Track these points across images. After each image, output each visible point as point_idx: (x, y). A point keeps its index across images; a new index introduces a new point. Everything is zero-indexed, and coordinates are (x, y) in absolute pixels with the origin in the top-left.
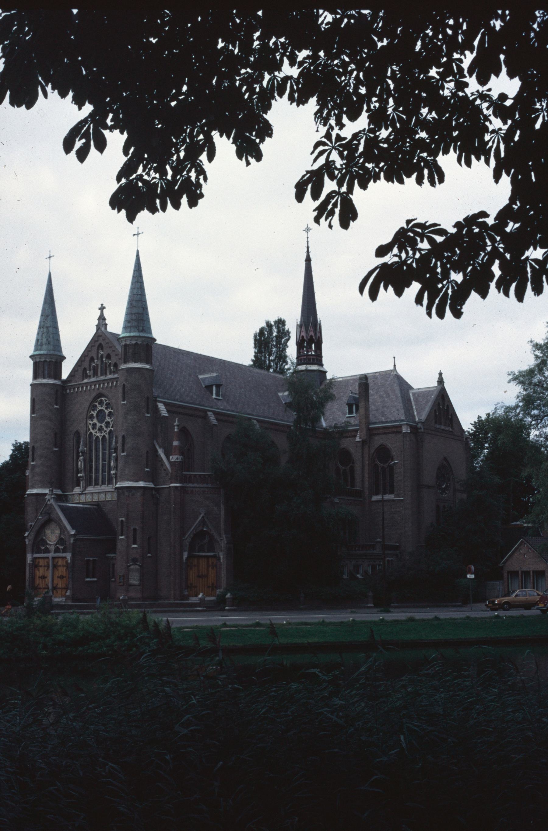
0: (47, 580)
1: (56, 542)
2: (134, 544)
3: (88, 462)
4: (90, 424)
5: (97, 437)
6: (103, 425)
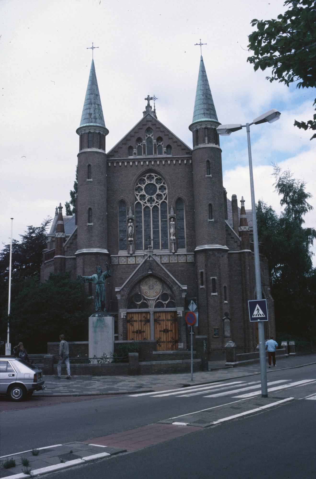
0: (144, 335)
1: (157, 297)
2: (226, 300)
3: (137, 229)
4: (137, 195)
6: (154, 197)
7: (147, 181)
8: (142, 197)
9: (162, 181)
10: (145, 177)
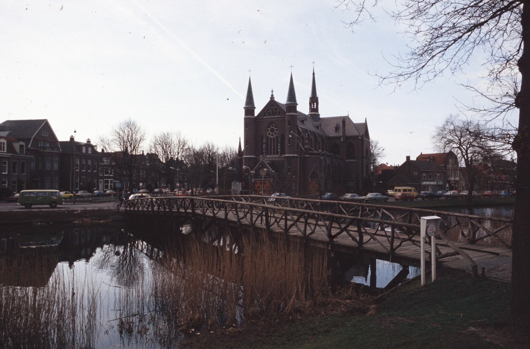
3: (267, 146)
5: (271, 138)
6: (274, 133)
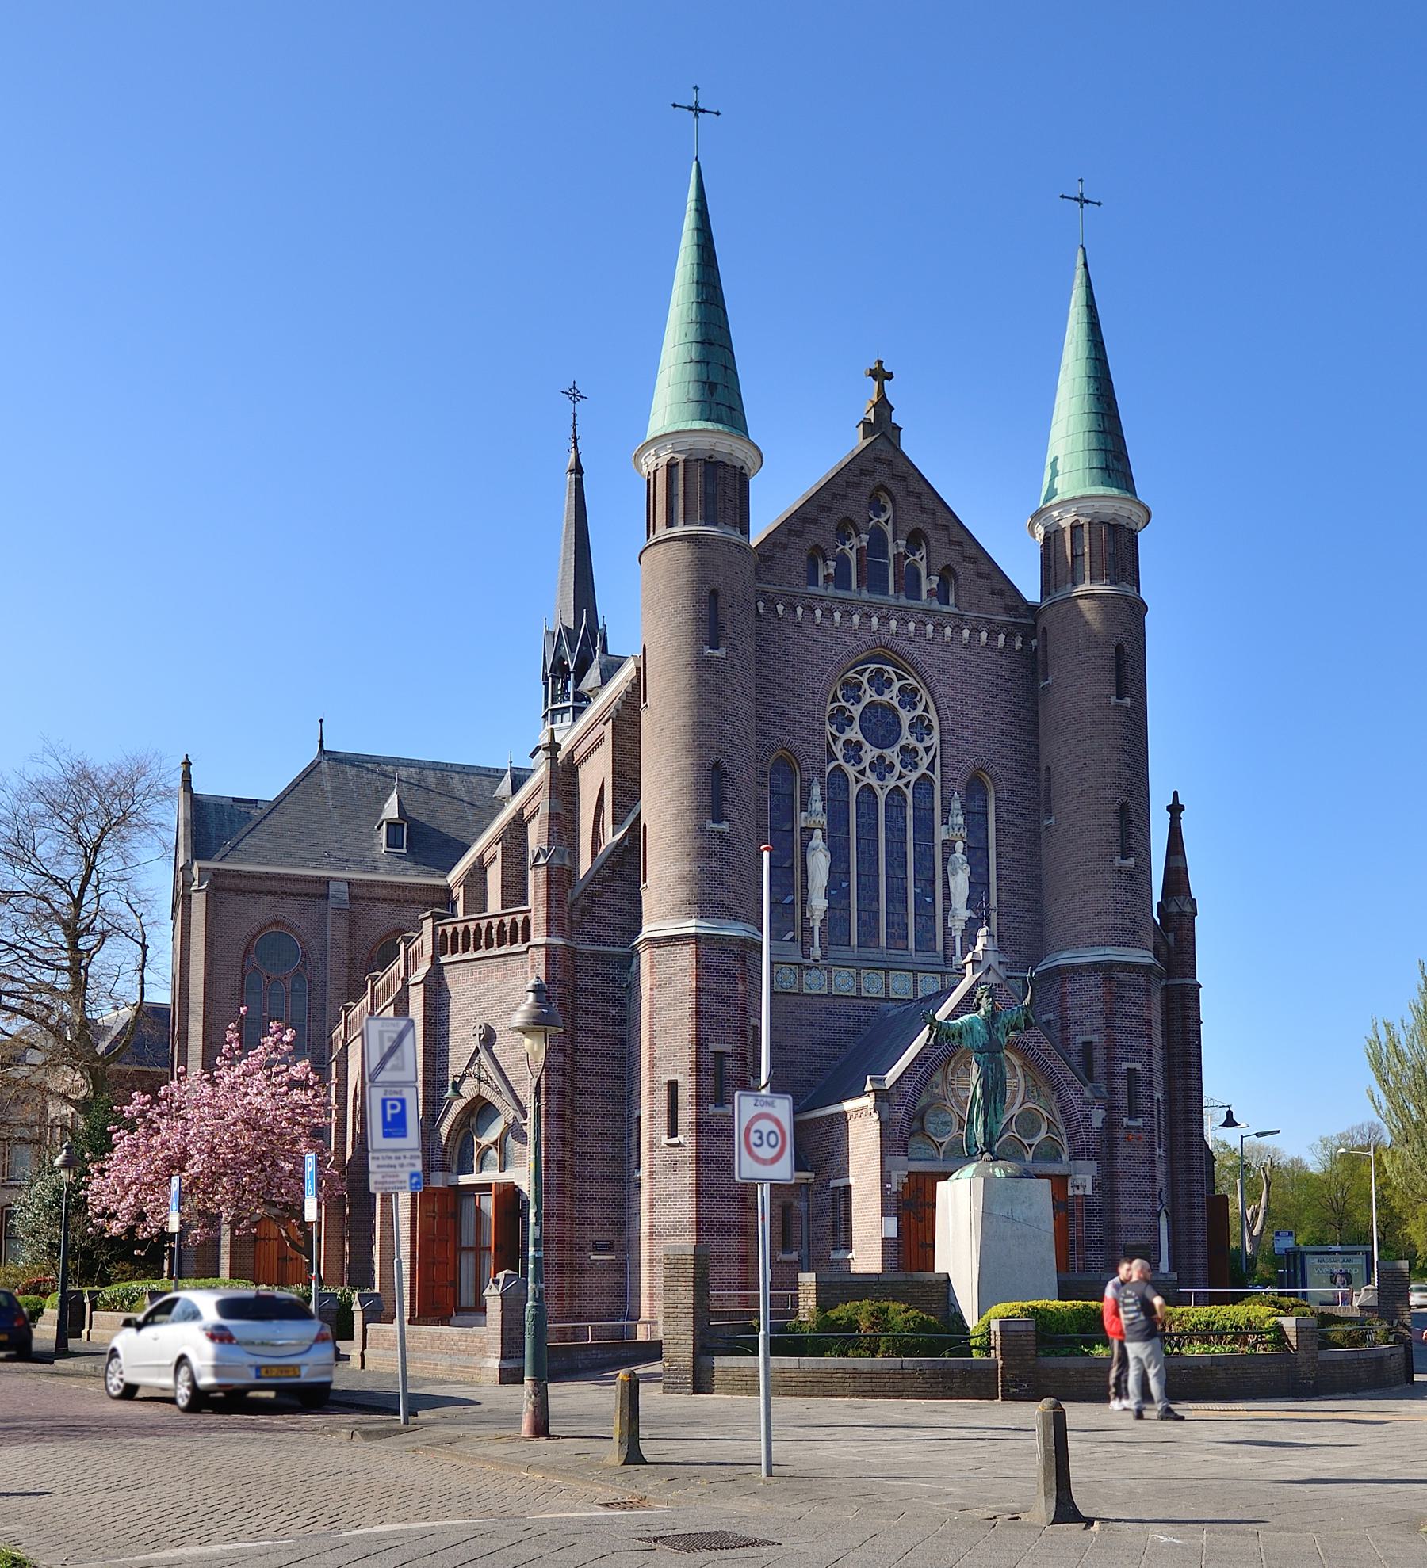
5: (869, 786)
6: (892, 755)
7: (868, 690)
8: (853, 750)
9: (921, 699)
10: (861, 673)
